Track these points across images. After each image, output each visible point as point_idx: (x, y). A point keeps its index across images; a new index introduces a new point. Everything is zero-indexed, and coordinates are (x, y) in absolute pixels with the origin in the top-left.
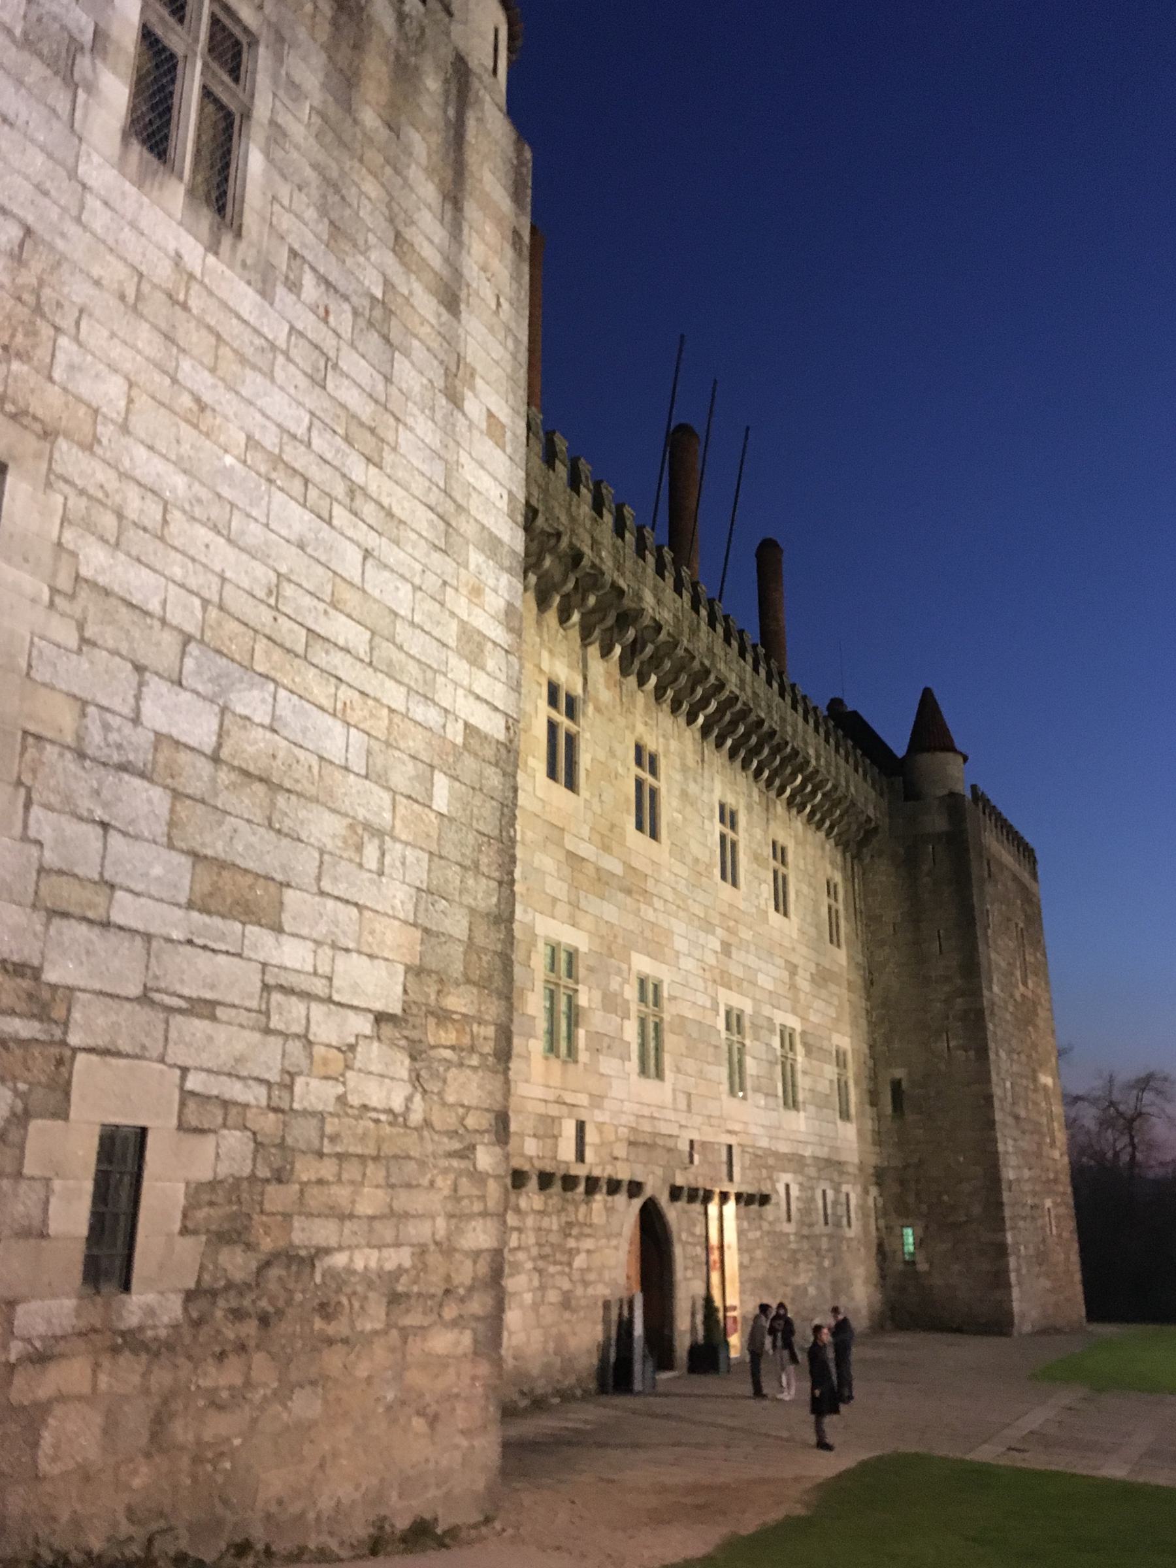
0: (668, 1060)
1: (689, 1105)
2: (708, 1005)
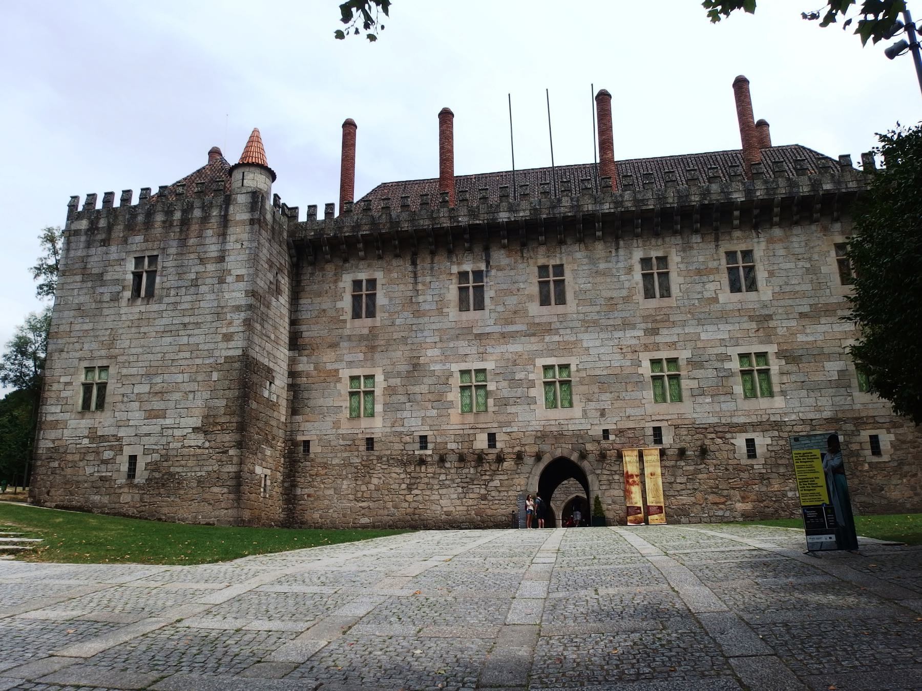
0: (575, 398)
1: (603, 413)
2: (628, 363)
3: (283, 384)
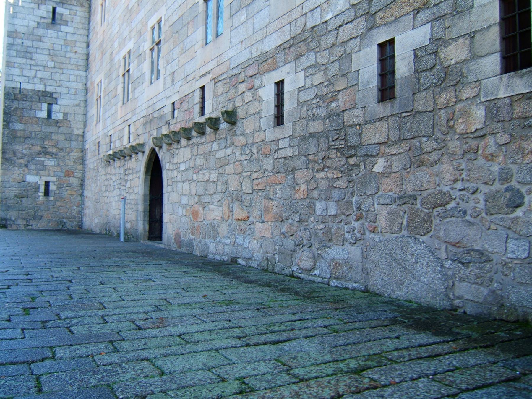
3: (76, 102)
